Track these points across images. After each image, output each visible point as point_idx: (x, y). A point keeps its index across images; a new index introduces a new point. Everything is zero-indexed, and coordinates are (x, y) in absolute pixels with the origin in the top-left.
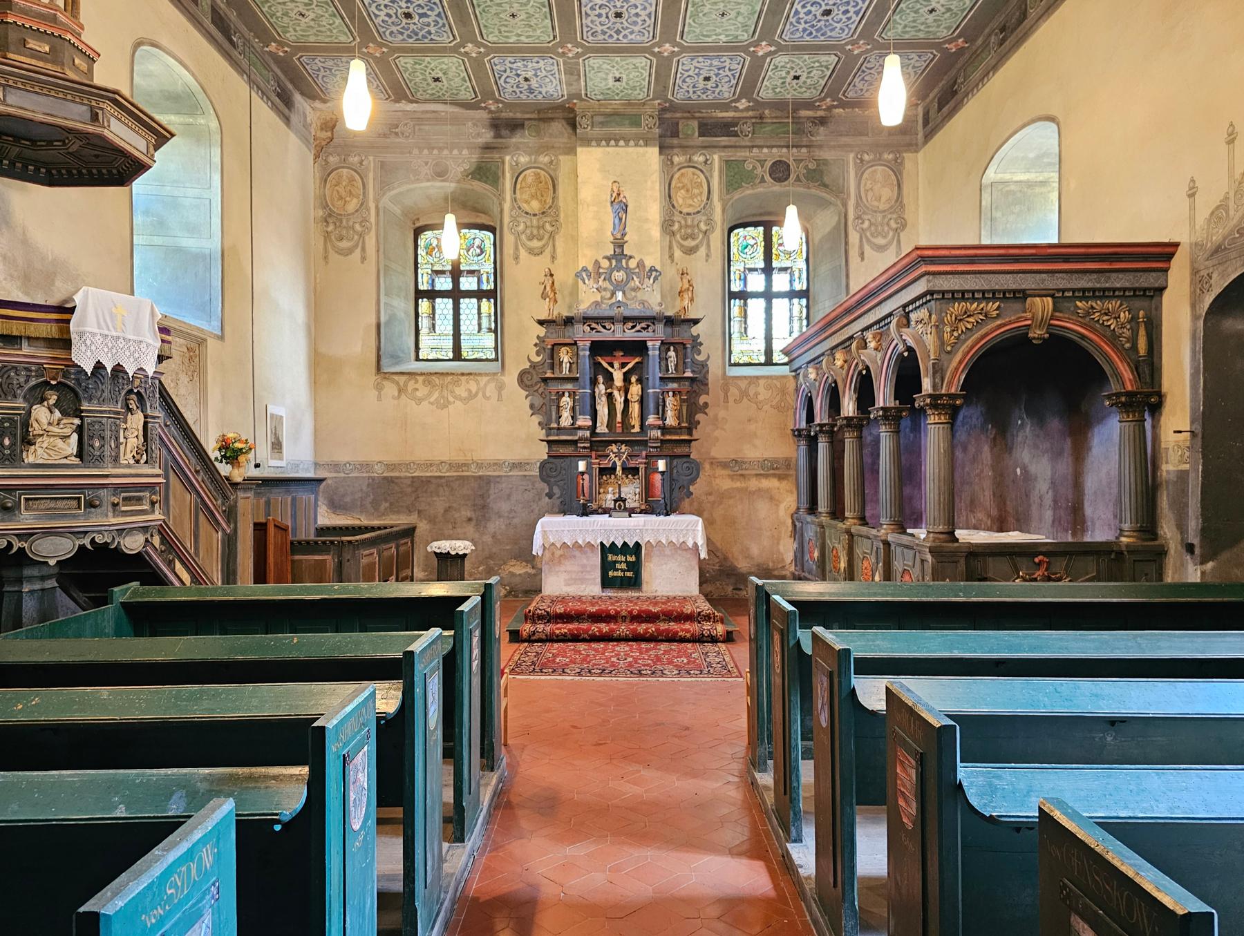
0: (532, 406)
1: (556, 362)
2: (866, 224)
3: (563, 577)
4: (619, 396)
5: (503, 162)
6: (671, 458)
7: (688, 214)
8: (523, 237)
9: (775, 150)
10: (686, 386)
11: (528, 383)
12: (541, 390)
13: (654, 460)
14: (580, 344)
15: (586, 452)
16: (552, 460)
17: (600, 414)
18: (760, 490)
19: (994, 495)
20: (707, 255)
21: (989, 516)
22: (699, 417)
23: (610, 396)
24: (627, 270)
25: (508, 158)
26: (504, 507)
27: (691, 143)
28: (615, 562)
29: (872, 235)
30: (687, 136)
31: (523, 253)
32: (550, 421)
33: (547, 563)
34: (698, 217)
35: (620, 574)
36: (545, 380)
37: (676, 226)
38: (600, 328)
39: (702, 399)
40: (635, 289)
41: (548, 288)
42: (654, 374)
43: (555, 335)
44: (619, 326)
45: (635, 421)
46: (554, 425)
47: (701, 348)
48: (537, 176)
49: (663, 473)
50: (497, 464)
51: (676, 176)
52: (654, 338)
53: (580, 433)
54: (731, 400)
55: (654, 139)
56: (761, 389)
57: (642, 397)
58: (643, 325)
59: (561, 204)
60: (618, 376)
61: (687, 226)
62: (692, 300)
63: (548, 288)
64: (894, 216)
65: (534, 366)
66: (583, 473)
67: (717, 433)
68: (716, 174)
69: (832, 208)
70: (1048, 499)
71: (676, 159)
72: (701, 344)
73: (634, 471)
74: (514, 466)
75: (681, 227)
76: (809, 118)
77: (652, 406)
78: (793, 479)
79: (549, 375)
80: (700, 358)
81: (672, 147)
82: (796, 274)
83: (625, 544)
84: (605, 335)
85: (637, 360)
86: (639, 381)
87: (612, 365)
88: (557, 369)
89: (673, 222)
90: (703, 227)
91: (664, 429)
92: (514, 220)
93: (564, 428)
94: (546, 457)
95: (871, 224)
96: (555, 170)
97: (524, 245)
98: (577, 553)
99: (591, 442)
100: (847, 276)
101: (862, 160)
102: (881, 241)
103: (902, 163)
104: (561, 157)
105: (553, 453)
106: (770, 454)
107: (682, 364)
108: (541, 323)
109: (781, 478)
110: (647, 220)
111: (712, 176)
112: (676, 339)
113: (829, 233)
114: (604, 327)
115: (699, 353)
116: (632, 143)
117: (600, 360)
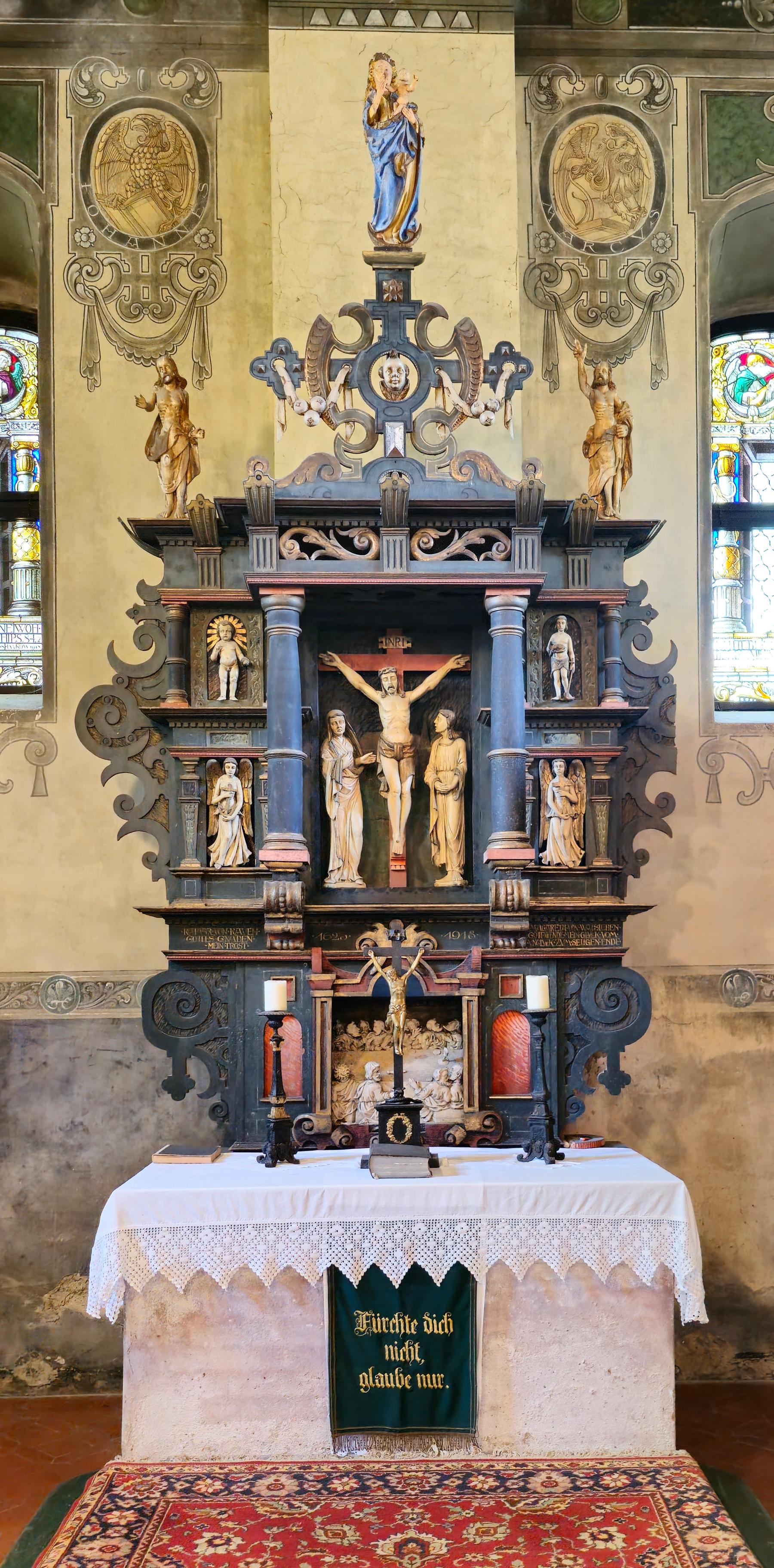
0: (122, 805)
1: (198, 662)
4: (398, 780)
5: (51, 88)
6: (562, 967)
7: (601, 248)
10: (606, 741)
11: (100, 722)
12: (150, 755)
13: (509, 971)
14: (271, 598)
15: (292, 949)
17: (338, 830)
22: (645, 839)
23: (369, 776)
24: (424, 357)
25: (64, 75)
27: (606, 42)
28: (381, 1339)
30: (597, 22)
31: (110, 356)
32: (177, 850)
33: (141, 1346)
34: (628, 258)
36: (162, 721)
37: (565, 284)
39: (656, 785)
40: (442, 419)
42: (508, 699)
44: (393, 541)
45: (448, 854)
46: (192, 864)
47: (653, 626)
48: (154, 129)
49: (538, 1018)
51: (564, 137)
52: (509, 574)
53: (271, 890)
54: (728, 792)
55: (501, 9)
57: (468, 778)
58: (475, 537)
59: (224, 210)
60: (394, 713)
61: (596, 284)
62: (626, 467)
65: (128, 678)
66: (277, 1020)
67: (688, 893)
68: (681, 133)
72: (651, 613)
73: (446, 1010)
75: (578, 286)
77: (501, 801)
79: (173, 702)
80: (650, 656)
81: (551, 52)
83: (416, 1273)
85: (452, 664)
86: (460, 728)
87: (373, 678)
88: (199, 688)
89: (557, 270)
90: (645, 288)
91: (540, 877)
93: (224, 874)
94: (163, 964)
96: (206, 112)
98: (247, 1308)
99: (308, 918)
104: (224, 75)
105: (185, 954)
107: (595, 666)
108: (149, 535)
110: (480, 250)
111: (669, 139)
112: (577, 592)
115: (645, 641)
116: (434, 20)
117: (338, 662)
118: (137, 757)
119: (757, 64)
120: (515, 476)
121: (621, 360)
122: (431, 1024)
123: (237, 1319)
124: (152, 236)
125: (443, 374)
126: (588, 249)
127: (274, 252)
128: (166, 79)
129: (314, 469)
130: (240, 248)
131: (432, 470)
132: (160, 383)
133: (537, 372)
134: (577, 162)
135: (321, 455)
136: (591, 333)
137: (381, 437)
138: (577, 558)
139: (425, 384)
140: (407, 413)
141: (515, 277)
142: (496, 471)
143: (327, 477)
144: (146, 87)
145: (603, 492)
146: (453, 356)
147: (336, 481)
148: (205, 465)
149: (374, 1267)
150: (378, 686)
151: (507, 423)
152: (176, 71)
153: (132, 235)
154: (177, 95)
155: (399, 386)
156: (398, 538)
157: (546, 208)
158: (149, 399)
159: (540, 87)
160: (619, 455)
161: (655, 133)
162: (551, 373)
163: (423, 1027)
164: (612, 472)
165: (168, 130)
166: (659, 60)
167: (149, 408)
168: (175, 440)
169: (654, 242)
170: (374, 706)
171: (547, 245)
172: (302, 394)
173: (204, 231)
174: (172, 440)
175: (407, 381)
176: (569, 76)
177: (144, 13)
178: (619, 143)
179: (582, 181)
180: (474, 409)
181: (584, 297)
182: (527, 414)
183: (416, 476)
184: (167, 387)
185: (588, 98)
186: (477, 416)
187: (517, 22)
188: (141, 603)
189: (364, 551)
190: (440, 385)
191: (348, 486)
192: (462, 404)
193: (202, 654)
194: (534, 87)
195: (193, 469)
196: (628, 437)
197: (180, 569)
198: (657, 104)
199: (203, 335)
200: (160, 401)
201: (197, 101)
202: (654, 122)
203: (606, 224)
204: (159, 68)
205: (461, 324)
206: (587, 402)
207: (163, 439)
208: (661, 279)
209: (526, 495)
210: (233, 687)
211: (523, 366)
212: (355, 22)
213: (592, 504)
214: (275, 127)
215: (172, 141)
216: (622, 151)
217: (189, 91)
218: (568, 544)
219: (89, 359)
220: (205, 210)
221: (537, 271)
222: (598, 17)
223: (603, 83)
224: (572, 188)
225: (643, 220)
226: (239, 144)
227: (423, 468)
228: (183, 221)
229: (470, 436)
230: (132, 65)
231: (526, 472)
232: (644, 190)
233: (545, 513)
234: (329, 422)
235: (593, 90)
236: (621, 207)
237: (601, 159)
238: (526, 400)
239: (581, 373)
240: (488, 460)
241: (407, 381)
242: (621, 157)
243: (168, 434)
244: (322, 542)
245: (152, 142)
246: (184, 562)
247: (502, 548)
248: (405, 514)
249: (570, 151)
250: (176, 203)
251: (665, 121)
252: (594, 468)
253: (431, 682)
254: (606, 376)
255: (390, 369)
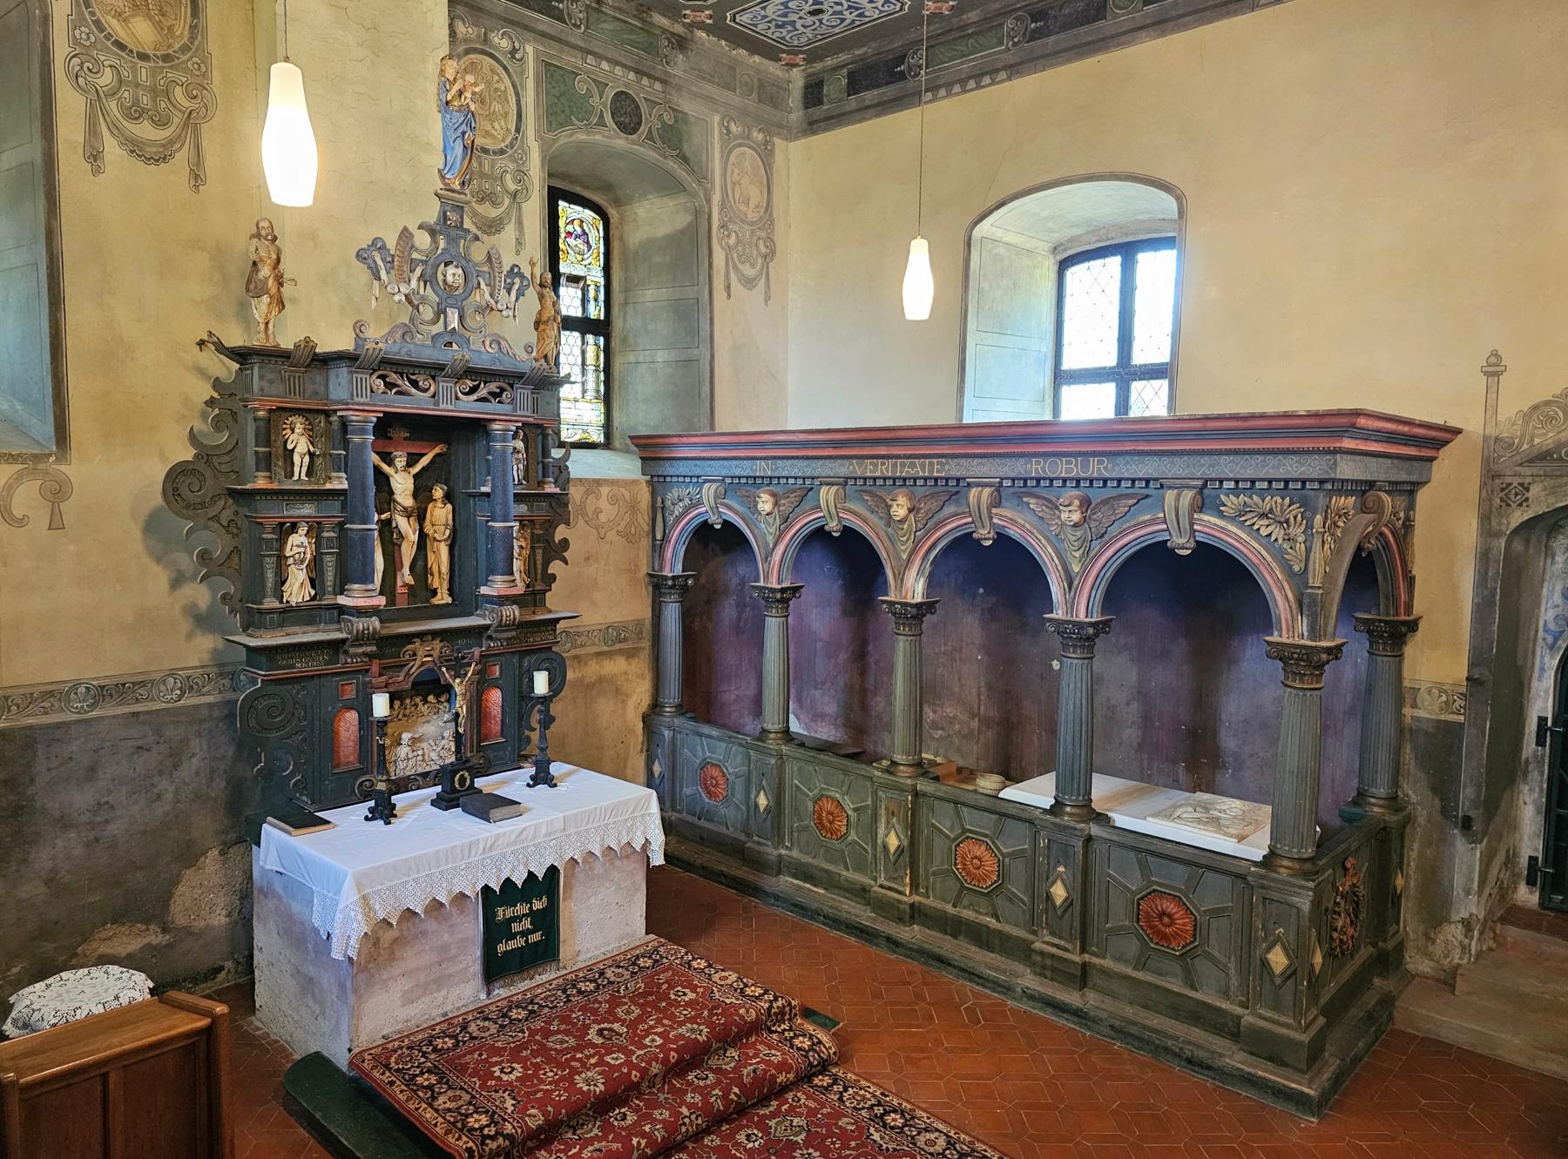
2: (732, 241)
3: (398, 988)
9: (618, 70)
16: (271, 689)
18: (601, 679)
19: (990, 688)
21: (973, 716)
22: (555, 567)
26: (80, 799)
29: (739, 257)
35: (519, 942)
38: (406, 385)
43: (278, 388)
46: (271, 603)
50: (53, 694)
56: (604, 504)
57: (454, 532)
59: (213, 46)
60: (402, 485)
61: (483, 175)
64: (764, 235)
68: (530, 83)
69: (682, 199)
70: (1132, 712)
74: (102, 693)
76: (664, 31)
78: (645, 655)
82: (592, 294)
84: (417, 402)
85: (437, 450)
86: (448, 497)
93: (298, 608)
95: (738, 240)
97: (114, 128)
98: (431, 925)
100: (712, 319)
101: (729, 132)
102: (749, 271)
103: (771, 152)
106: (614, 617)
109: (630, 654)
111: (524, 87)
113: (667, 237)
114: (415, 384)
118: (216, 518)
119: (573, 52)
122: (431, 698)
123: (424, 933)
124: (151, 53)
136: (480, 208)
149: (508, 879)
150: (390, 463)
153: (131, 46)
163: (425, 701)
170: (387, 477)
188: (216, 395)
193: (280, 443)
197: (271, 382)
199: (198, 147)
210: (304, 469)
219: (93, 147)
228: (177, 46)
236: (496, 125)
246: (273, 376)
250: (170, 28)
253: (424, 461)
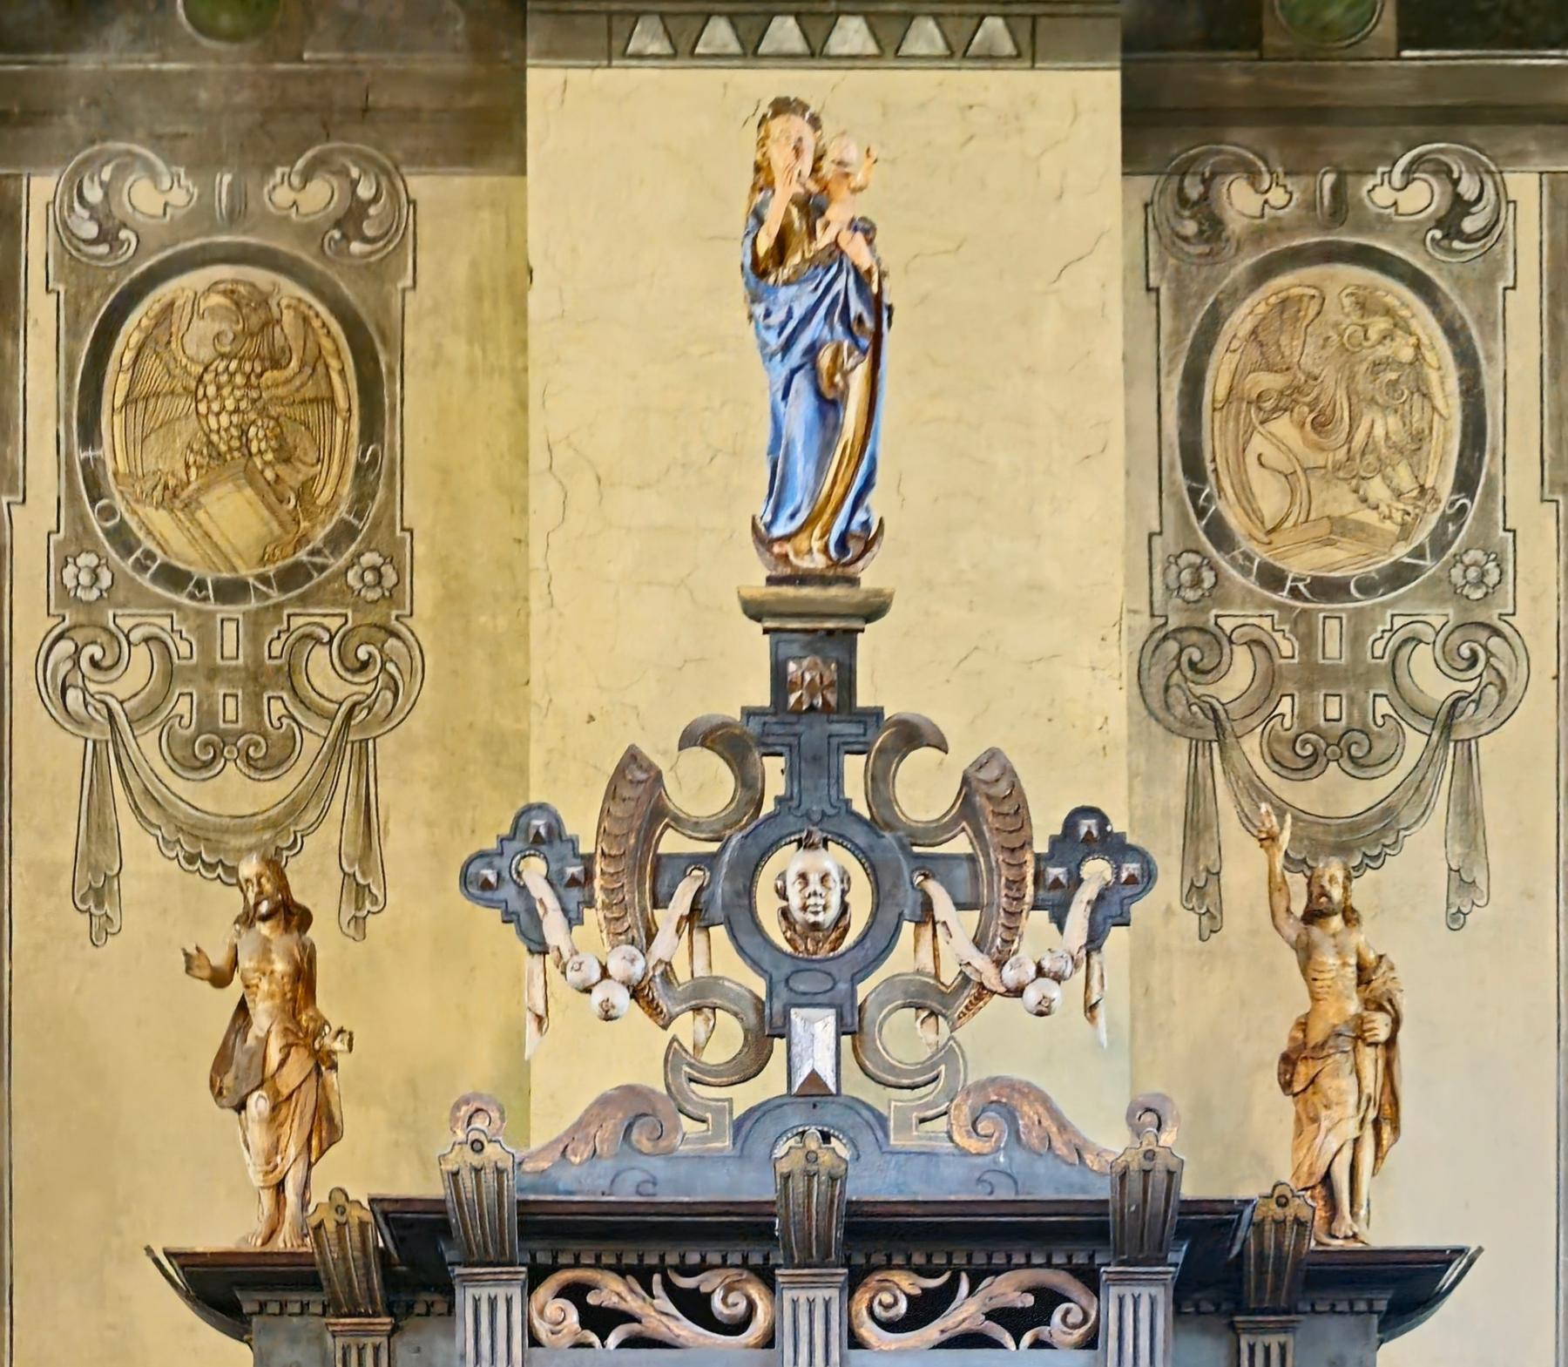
8: (147, 746)
20: (1461, 881)
25: (42, 189)
41: (263, 1017)
48: (252, 310)
51: (1240, 321)
63: (263, 1017)
71: (1241, 201)
90: (1432, 682)
92: (80, 619)
96: (378, 272)
104: (420, 185)
120: (1112, 1142)
121: (1374, 861)
125: (934, 888)
126: (1295, 593)
127: (535, 605)
128: (283, 196)
129: (613, 1124)
130: (454, 597)
131: (904, 1127)
132: (248, 919)
133: (1169, 885)
134: (1269, 381)
135: (631, 1091)
137: (779, 1045)
138: (1260, 1341)
139: (889, 916)
140: (843, 986)
141: (1119, 660)
142: (1063, 1126)
143: (646, 1145)
144: (235, 216)
145: (1327, 1179)
146: (960, 844)
147: (668, 1154)
148: (349, 1115)
151: (1091, 1008)
152: (307, 177)
154: (309, 232)
155: (826, 918)
156: (820, 1295)
157: (1194, 494)
158: (219, 958)
159: (1183, 200)
160: (1370, 1086)
161: (1462, 307)
162: (1203, 891)
164: (1350, 1129)
165: (288, 317)
166: (1473, 132)
167: (220, 979)
168: (285, 1059)
169: (1457, 573)
171: (1197, 582)
172: (587, 941)
173: (369, 558)
174: (274, 1057)
175: (844, 908)
176: (1253, 176)
177: (234, 37)
178: (1373, 334)
179: (1283, 426)
180: (1010, 975)
181: (1285, 706)
182: (1143, 990)
183: (866, 1139)
184: (264, 929)
185: (1299, 227)
186: (1018, 992)
187: (1128, 45)
189: (737, 1327)
190: (926, 914)
191: (699, 1165)
192: (981, 962)
194: (1169, 202)
195: (325, 1127)
196: (1391, 1043)
198: (1469, 239)
200: (245, 963)
201: (356, 247)
202: (1457, 281)
203: (1341, 528)
204: (268, 169)
205: (980, 765)
206: (1291, 958)
207: (252, 1055)
208: (1473, 661)
209: (1135, 1184)
211: (1131, 868)
212: (734, 47)
213: (1297, 1208)
214: (538, 301)
215: (297, 346)
216: (1382, 351)
217: (338, 224)
218: (1240, 1308)
220: (373, 509)
221: (1172, 647)
222: (1325, 29)
223: (1337, 190)
224: (1258, 444)
225: (1432, 520)
226: (457, 348)
227: (882, 1120)
229: (996, 1042)
230: (202, 164)
231: (1138, 1133)
232: (1434, 446)
233: (1182, 1232)
234: (652, 1008)
235: (1311, 205)
236: (1377, 489)
237: (1328, 374)
238: (1143, 956)
239: (1275, 887)
240: (1045, 1101)
241: (844, 908)
242: (1377, 366)
243: (264, 1042)
244: (633, 1304)
245: (249, 347)
247: (1076, 1317)
248: (837, 1234)
249: (1254, 353)
251: (1489, 280)
252: (1307, 1120)
254: (1337, 893)
255: (803, 877)
